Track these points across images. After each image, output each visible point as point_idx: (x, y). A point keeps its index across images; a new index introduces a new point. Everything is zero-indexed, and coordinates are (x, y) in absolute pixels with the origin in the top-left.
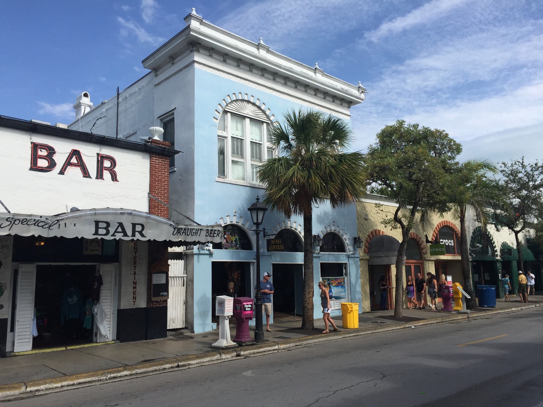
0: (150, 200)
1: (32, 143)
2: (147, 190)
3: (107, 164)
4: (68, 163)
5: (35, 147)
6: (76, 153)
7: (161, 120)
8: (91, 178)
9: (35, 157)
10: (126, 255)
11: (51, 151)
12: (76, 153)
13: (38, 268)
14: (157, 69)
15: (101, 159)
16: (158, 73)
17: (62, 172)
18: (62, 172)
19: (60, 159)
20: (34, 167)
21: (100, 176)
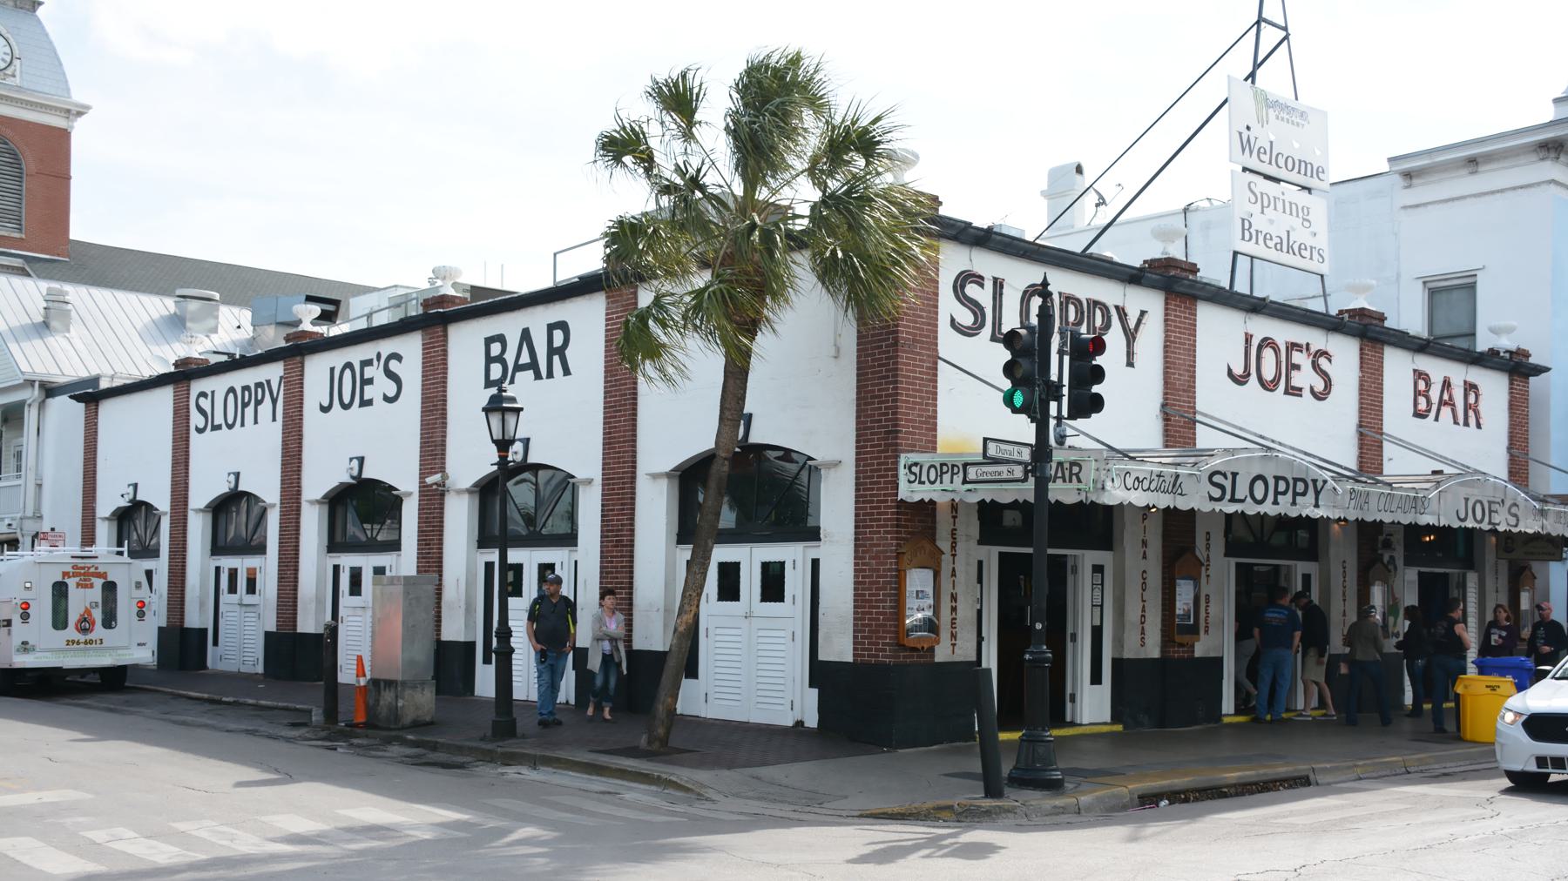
0: (1510, 460)
1: (1415, 371)
2: (1504, 442)
3: (1472, 399)
4: (1442, 403)
5: (1419, 375)
6: (1447, 384)
7: (1425, 283)
8: (1458, 424)
9: (1417, 393)
10: (1130, 537)
11: (1428, 384)
12: (1447, 384)
13: (1420, 574)
14: (1412, 174)
15: (1470, 387)
16: (1415, 181)
17: (1437, 419)
18: (1437, 419)
19: (1435, 394)
20: (1419, 415)
21: (1466, 424)
